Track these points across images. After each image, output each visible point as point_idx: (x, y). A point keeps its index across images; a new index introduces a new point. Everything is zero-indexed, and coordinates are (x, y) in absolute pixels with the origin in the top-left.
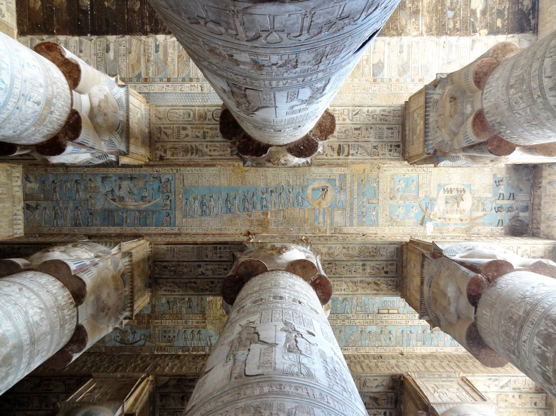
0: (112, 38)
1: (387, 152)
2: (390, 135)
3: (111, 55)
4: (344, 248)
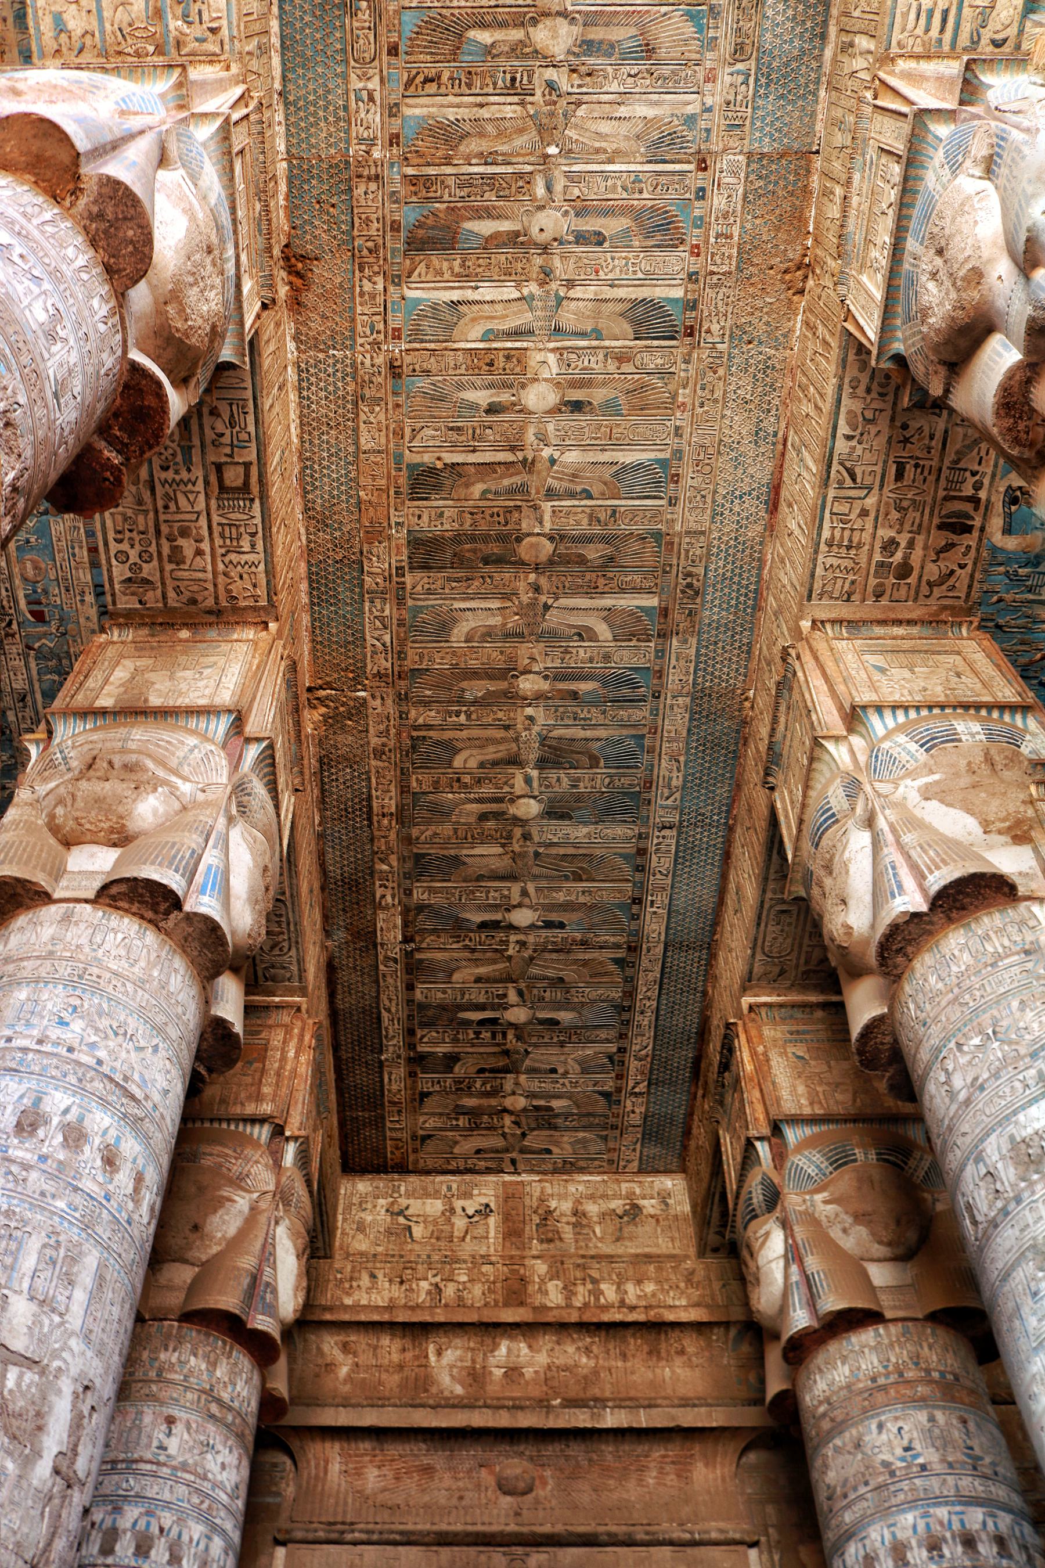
3: (565, 1016)
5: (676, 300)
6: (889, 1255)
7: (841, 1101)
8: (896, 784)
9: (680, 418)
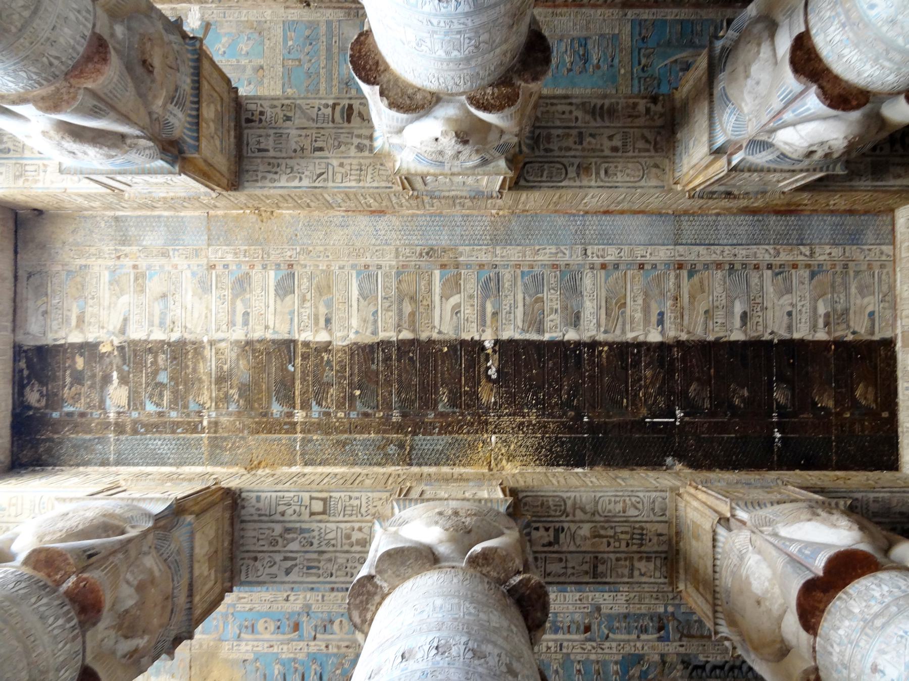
0: (737, 336)
1: (269, 112)
2: (262, 139)
3: (738, 308)
5: (276, 275)
9: (335, 267)
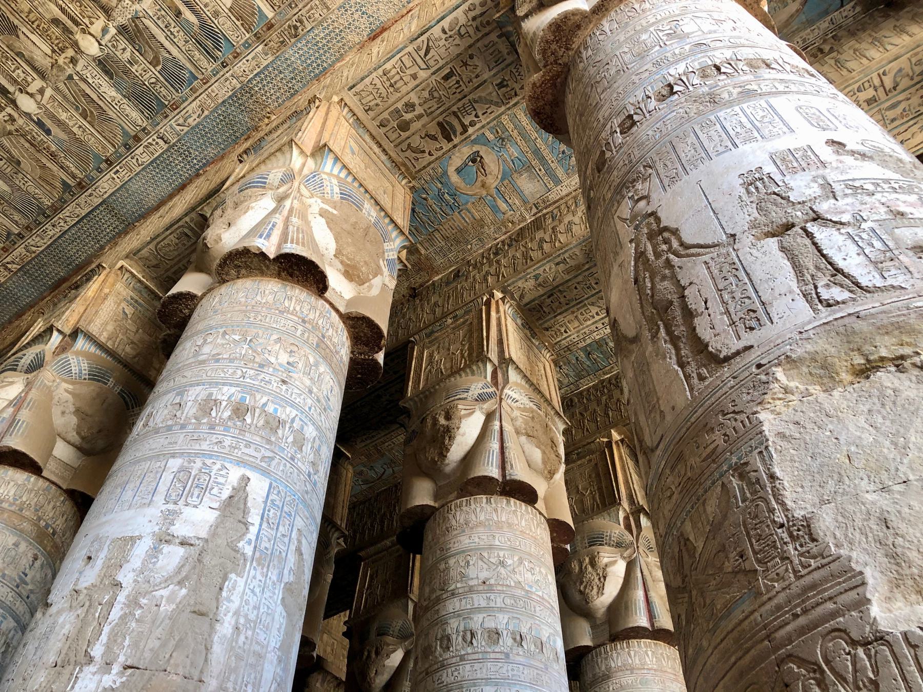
4: (558, 264)
6: (77, 443)
7: (127, 351)
8: (312, 196)
